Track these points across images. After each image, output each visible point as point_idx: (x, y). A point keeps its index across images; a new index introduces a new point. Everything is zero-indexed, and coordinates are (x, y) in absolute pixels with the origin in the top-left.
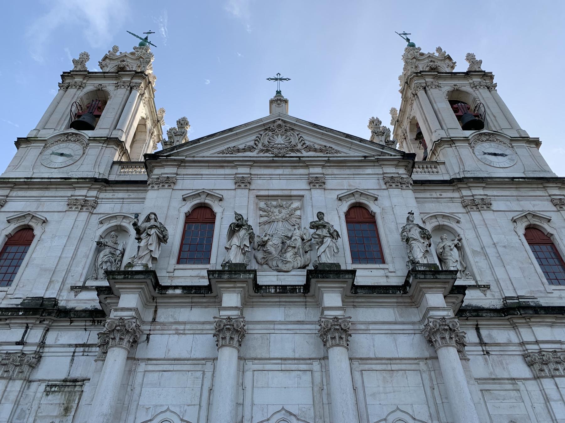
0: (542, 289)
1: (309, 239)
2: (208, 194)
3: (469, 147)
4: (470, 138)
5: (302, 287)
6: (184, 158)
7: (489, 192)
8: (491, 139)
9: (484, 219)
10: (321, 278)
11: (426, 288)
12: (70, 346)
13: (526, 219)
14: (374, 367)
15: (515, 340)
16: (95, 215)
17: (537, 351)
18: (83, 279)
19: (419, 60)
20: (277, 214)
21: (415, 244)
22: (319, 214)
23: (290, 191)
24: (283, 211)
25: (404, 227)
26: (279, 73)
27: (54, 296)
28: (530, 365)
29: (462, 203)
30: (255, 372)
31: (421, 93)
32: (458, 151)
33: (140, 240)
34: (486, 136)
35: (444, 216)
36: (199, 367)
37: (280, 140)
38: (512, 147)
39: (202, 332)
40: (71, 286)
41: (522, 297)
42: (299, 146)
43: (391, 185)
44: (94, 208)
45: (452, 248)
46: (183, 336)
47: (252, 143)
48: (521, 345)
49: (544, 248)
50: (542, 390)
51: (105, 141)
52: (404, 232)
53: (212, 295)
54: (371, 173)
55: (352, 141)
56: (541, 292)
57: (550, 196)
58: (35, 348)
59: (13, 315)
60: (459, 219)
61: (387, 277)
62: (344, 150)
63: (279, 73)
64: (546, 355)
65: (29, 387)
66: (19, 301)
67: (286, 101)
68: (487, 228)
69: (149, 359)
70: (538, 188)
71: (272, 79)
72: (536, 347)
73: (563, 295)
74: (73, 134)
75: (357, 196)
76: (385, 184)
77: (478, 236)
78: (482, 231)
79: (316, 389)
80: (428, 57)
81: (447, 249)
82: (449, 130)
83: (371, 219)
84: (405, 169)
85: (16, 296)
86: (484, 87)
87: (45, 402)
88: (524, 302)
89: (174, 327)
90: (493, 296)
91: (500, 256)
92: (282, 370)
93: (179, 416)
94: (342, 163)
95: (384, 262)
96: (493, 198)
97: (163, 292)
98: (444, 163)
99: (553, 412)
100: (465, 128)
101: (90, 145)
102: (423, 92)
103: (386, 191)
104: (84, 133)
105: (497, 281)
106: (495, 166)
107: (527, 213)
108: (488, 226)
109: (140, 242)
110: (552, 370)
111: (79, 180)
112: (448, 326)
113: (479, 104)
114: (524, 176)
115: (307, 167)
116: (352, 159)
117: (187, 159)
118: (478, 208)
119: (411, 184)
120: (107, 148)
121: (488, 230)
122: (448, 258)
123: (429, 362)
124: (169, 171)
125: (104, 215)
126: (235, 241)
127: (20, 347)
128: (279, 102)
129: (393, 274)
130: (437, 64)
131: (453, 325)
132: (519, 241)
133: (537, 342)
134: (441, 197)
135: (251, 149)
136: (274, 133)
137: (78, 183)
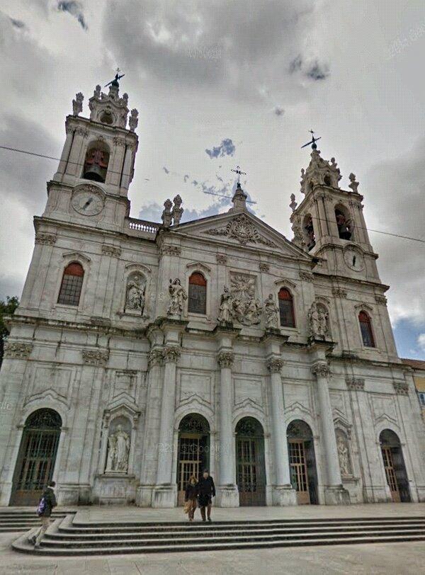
7: (347, 287)
15: (343, 372)
18: (123, 307)
20: (243, 287)
24: (244, 284)
28: (348, 384)
31: (320, 202)
37: (243, 230)
39: (207, 356)
41: (351, 351)
42: (254, 238)
47: (224, 229)
50: (351, 396)
77: (337, 313)
78: (340, 310)
83: (291, 299)
89: (194, 351)
94: (278, 257)
95: (294, 326)
105: (341, 341)
115: (259, 255)
124: (175, 242)
126: (225, 306)
127: (97, 348)
135: (225, 234)
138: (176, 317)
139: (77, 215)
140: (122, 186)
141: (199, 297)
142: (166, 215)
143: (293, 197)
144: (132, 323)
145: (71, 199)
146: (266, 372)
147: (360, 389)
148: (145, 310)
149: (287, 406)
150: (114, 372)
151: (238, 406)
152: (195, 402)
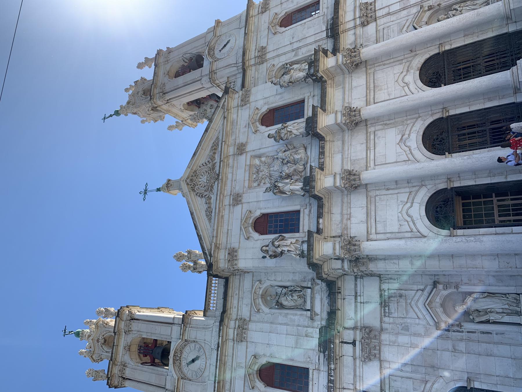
0: (322, 17)
1: (285, 145)
2: (245, 221)
5: (321, 142)
6: (213, 244)
8: (213, 49)
9: (273, 50)
10: (317, 125)
12: (356, 306)
14: (372, 97)
16: (251, 318)
18: (305, 313)
22: (270, 137)
23: (246, 166)
24: (262, 168)
25: (281, 86)
26: (140, 193)
27: (318, 330)
29: (260, 64)
30: (376, 164)
32: (220, 68)
33: (283, 251)
36: (373, 199)
37: (203, 179)
40: (311, 319)
42: (210, 165)
44: (245, 320)
46: (352, 214)
49: (294, 18)
50: (383, 16)
51: (184, 326)
53: (324, 198)
55: (210, 128)
56: (323, 19)
58: (358, 332)
59: (333, 352)
60: (271, 65)
61: (314, 96)
63: (140, 193)
65: (387, 329)
66: (322, 355)
67: (169, 180)
68: (279, 48)
69: (368, 232)
71: (145, 197)
73: (326, 7)
74: (174, 355)
77: (285, 54)
78: (280, 51)
79: (386, 127)
82: (202, 75)
85: (317, 361)
87: (397, 314)
88: (330, 26)
89: (345, 221)
90: (325, 44)
91: (299, 40)
92: (374, 149)
93: (404, 205)
95: (303, 101)
97: (321, 231)
99: (395, 11)
100: (201, 66)
101: (186, 339)
104: (173, 350)
105: (316, 42)
108: (278, 48)
109: (285, 251)
111: (221, 335)
113: (183, 57)
117: (214, 241)
120: (191, 324)
121: (281, 48)
123: (368, 67)
125: (252, 307)
127: (357, 343)
128: (169, 185)
129: (312, 93)
133: (354, 19)
136: (197, 184)
137: (222, 337)
138: (305, 247)
139: (206, 374)
140: (171, 321)
141: (281, 221)
142: (195, 269)
143: (170, 128)
144: (321, 299)
145: (190, 380)
146: (362, 126)
147: (373, 6)
148: (305, 284)
149: (404, 94)
150: (386, 319)
151: (410, 156)
152: (411, 212)
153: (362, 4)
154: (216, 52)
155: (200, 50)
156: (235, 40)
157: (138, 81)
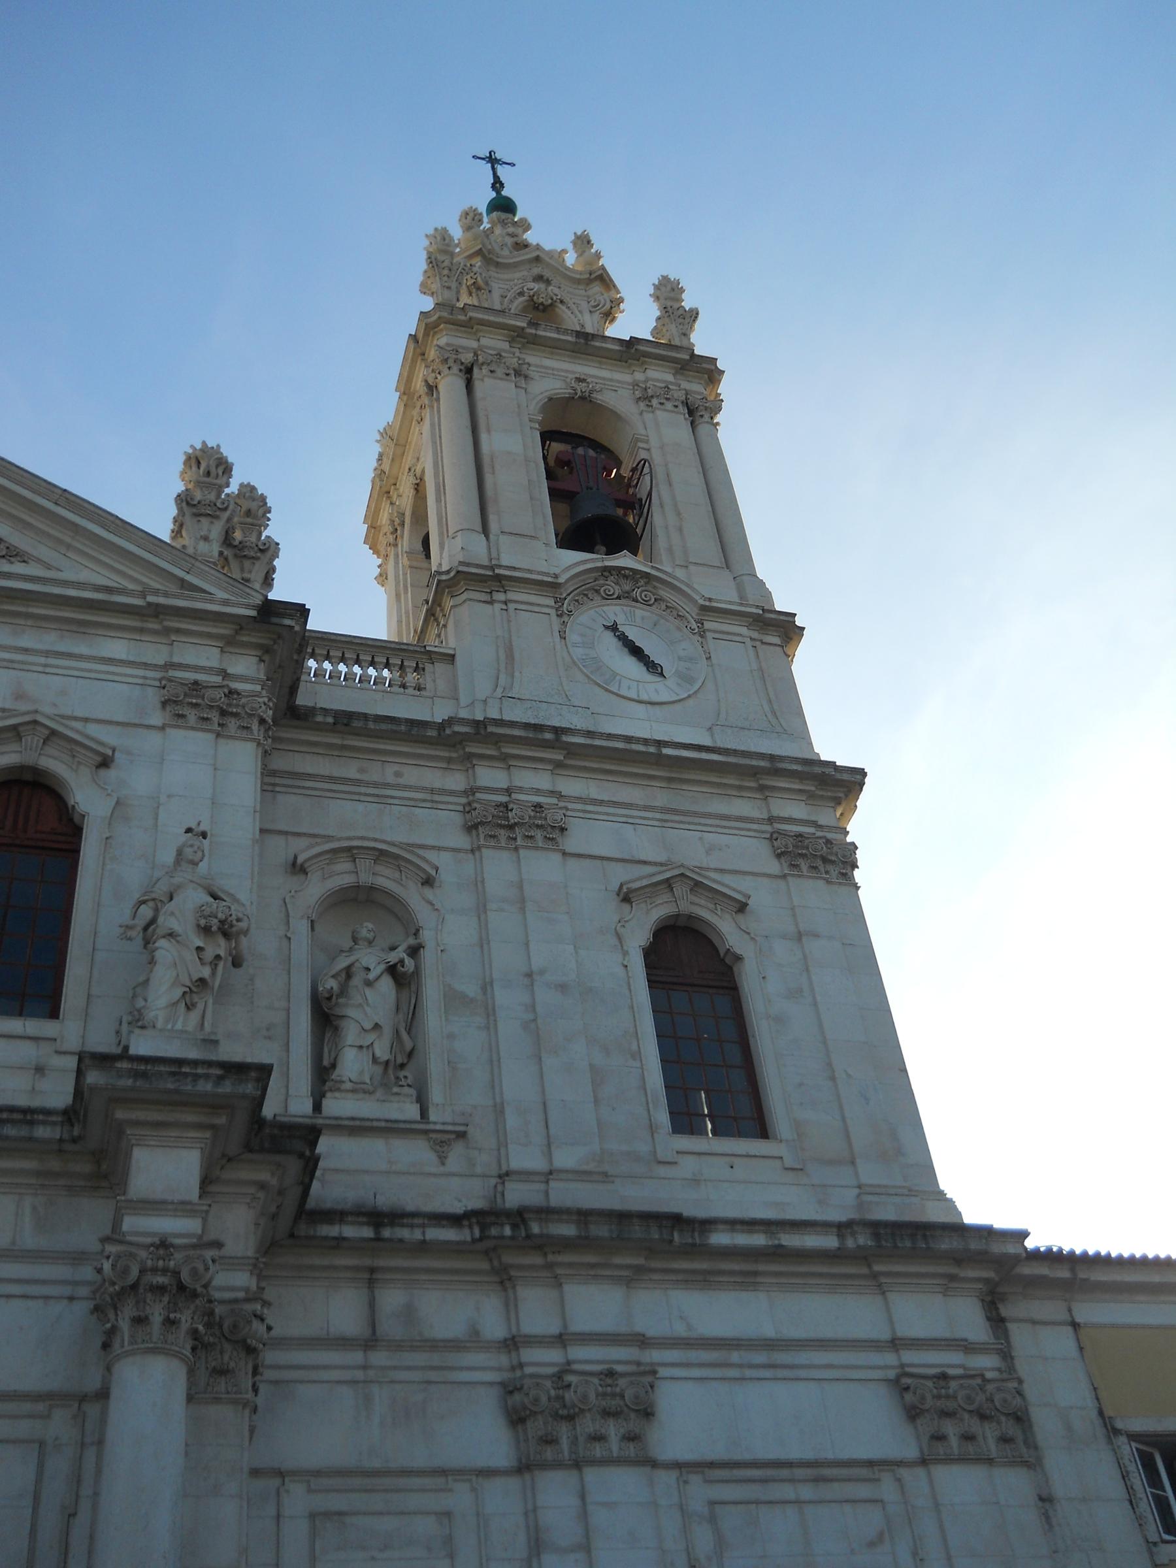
3: (553, 612)
4: (561, 580)
7: (572, 786)
8: (637, 593)
11: (137, 1123)
13: (666, 897)
17: (550, 1370)
19: (498, 264)
21: (165, 950)
28: (517, 1419)
31: (450, 386)
34: (622, 581)
35: (382, 853)
38: (702, 634)
43: (182, 716)
45: (372, 976)
48: (507, 1346)
50: (531, 1513)
52: (144, 902)
54: (124, 657)
57: (771, 820)
60: (433, 873)
62: (44, 552)
64: (577, 1386)
70: (740, 788)
72: (553, 1356)
75: (32, 740)
76: (164, 704)
77: (483, 943)
80: (530, 261)
81: (356, 981)
84: (261, 660)
86: (676, 406)
91: (535, 1020)
96: (580, 807)
98: (453, 656)
100: (572, 538)
102: (460, 384)
103: (155, 738)
106: (622, 693)
107: (676, 872)
110: (581, 1439)
112: (176, 1274)
114: (707, 742)
116: (57, 590)
118: (515, 839)
119: (262, 721)
122: (351, 1012)
130: (556, 291)
131: (194, 1272)
132: (620, 971)
134: (401, 781)
153: (650, 1379)
154: (616, 612)
155: (661, 543)
156: (655, 698)
157: (615, 286)
